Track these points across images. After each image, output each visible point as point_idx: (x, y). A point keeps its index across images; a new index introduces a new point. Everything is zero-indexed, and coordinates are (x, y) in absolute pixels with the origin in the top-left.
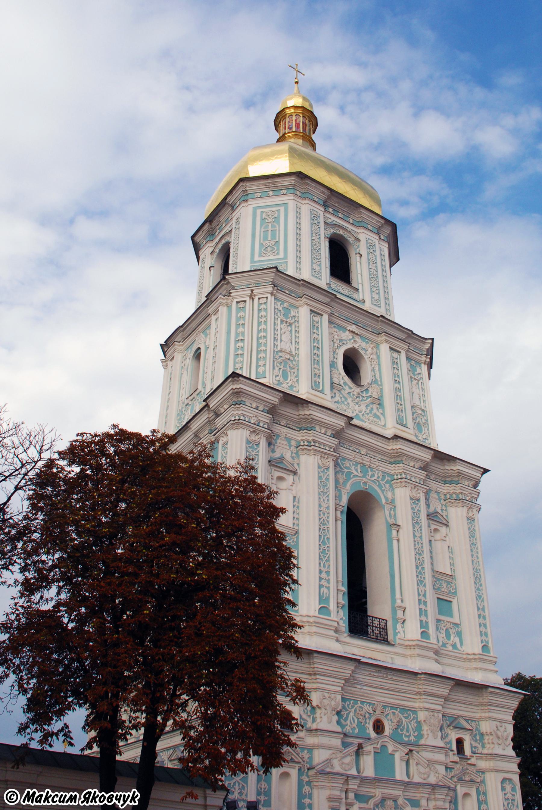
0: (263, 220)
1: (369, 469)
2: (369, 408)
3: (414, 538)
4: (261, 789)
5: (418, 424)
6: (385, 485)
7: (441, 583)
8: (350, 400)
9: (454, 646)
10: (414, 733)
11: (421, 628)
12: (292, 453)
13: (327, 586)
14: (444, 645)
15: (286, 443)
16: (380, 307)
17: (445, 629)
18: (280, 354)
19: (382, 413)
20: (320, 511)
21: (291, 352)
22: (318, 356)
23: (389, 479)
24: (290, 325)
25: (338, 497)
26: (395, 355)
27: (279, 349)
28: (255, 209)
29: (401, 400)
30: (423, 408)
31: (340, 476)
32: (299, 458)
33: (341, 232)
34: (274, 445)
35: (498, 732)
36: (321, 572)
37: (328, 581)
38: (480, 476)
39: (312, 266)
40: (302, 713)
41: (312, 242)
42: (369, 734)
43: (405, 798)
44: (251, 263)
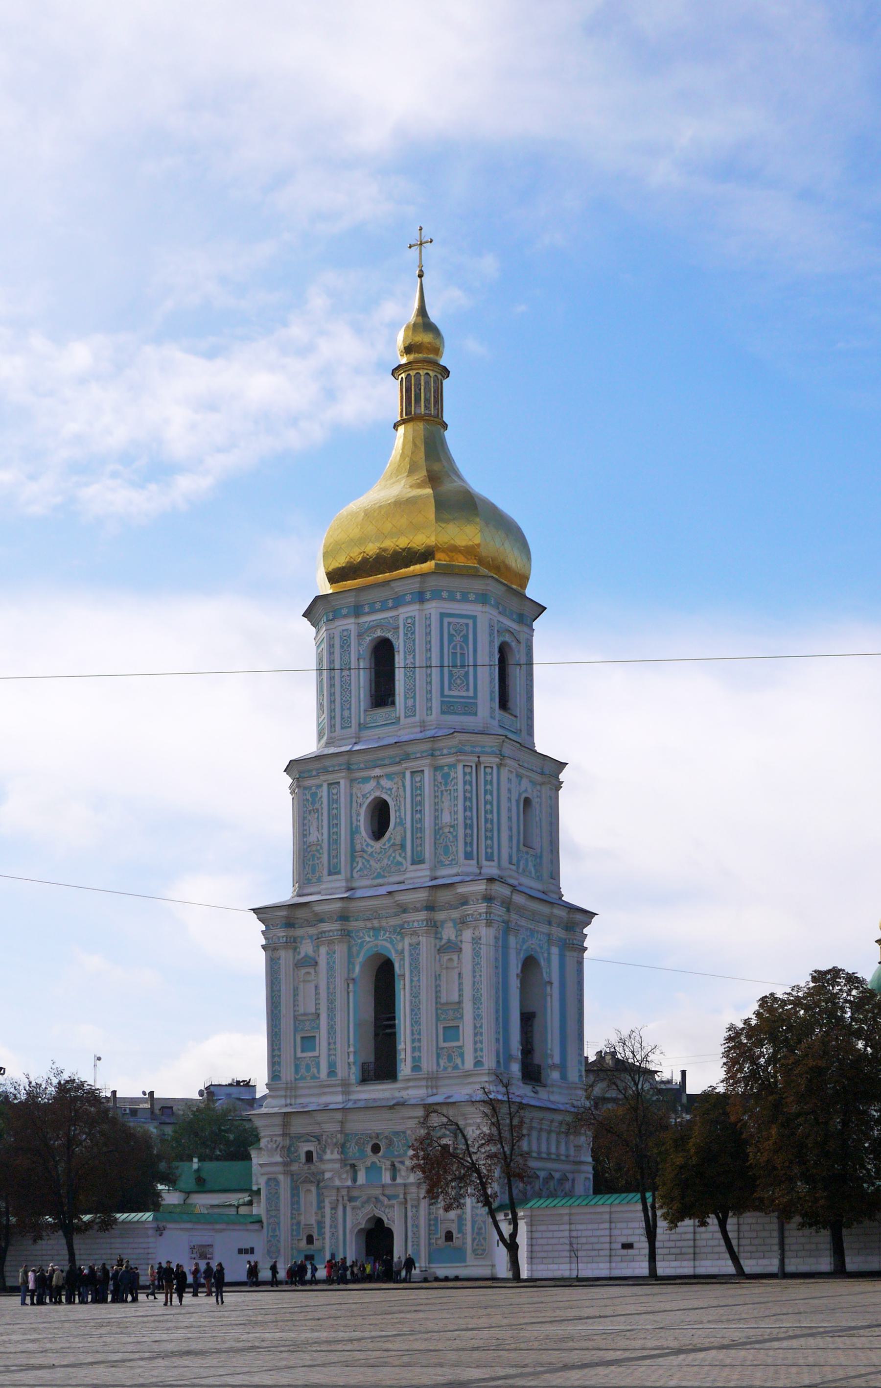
2: (392, 858)
8: (372, 863)
9: (456, 1067)
14: (445, 1069)
15: (309, 941)
16: (415, 715)
20: (328, 993)
21: (318, 841)
24: (318, 810)
26: (418, 779)
27: (308, 844)
31: (355, 949)
33: (379, 633)
36: (329, 1044)
37: (335, 1049)
39: (342, 715)
41: (342, 681)
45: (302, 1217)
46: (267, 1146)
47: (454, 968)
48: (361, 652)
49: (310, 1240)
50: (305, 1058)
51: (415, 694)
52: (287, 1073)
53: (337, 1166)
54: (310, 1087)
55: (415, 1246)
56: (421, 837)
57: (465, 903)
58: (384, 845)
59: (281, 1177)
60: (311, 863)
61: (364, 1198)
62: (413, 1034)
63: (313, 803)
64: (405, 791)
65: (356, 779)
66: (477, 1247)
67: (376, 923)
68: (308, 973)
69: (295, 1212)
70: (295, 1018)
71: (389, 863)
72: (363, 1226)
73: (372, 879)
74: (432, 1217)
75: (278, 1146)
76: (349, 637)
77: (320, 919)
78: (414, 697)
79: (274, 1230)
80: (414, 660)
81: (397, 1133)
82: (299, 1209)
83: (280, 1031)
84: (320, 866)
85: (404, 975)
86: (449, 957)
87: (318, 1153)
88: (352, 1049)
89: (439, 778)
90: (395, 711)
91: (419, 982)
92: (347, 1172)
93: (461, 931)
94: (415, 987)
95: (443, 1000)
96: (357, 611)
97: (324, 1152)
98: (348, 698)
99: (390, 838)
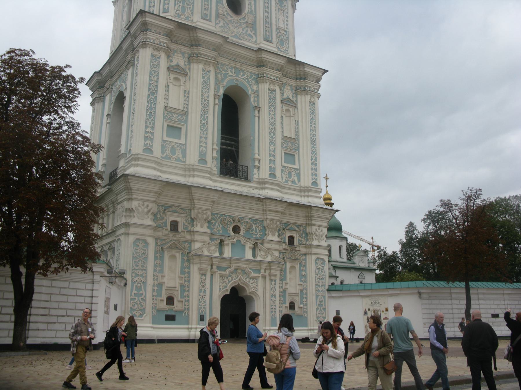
3: (269, 115)
4: (157, 264)
5: (282, 40)
7: (287, 144)
8: (230, 26)
9: (293, 182)
10: (260, 232)
12: (185, 62)
14: (287, 181)
15: (181, 55)
17: (288, 172)
19: (254, 34)
20: (202, 99)
25: (217, 89)
29: (269, 24)
30: (285, 29)
31: (219, 76)
32: (190, 65)
34: (172, 57)
35: (317, 232)
36: (201, 137)
37: (206, 143)
38: (321, 74)
40: (185, 222)
42: (230, 233)
43: (250, 269)
45: (165, 280)
46: (138, 210)
47: (291, 116)
49: (170, 300)
53: (207, 238)
54: (174, 167)
55: (274, 312)
56: (268, 27)
57: (305, 79)
58: (240, 20)
61: (233, 268)
62: (270, 151)
66: (319, 315)
67: (238, 65)
68: (176, 79)
69: (157, 274)
71: (244, 32)
72: (228, 293)
74: (281, 290)
77: (195, 43)
79: (138, 289)
81: (254, 220)
82: (161, 271)
85: (257, 108)
86: (287, 108)
87: (184, 224)
88: (215, 147)
91: (275, 116)
93: (296, 94)
94: (272, 118)
99: (244, 18)
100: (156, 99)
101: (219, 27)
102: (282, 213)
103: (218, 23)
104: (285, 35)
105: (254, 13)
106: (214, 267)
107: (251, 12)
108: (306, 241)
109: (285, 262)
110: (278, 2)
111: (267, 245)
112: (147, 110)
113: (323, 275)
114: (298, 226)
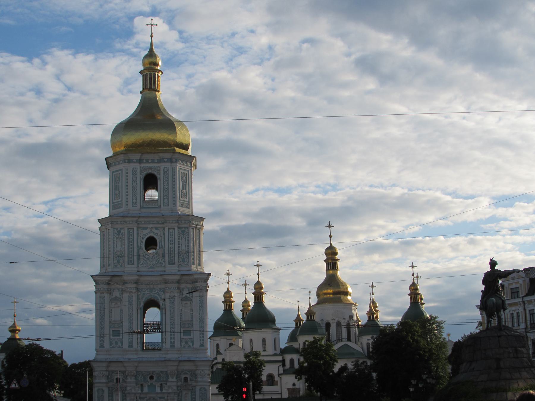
0: (115, 179)
1: (154, 289)
2: (157, 261)
6: (161, 293)
8: (148, 262)
9: (189, 346)
11: (171, 344)
12: (120, 293)
13: (132, 338)
14: (184, 347)
16: (168, 206)
18: (116, 253)
19: (163, 261)
20: (129, 313)
21: (121, 250)
22: (132, 248)
23: (163, 290)
24: (121, 238)
27: (116, 251)
28: (113, 172)
30: (186, 250)
33: (150, 171)
39: (133, 201)
41: (132, 188)
44: (113, 203)
48: (142, 178)
50: (115, 339)
51: (168, 197)
52: (107, 345)
53: (134, 384)
59: (104, 389)
60: (117, 259)
63: (119, 235)
64: (164, 234)
65: (140, 228)
67: (152, 286)
68: (116, 304)
70: (110, 322)
73: (148, 268)
75: (104, 375)
76: (137, 171)
77: (125, 283)
78: (168, 199)
80: (168, 184)
81: (162, 372)
83: (104, 327)
84: (122, 261)
87: (122, 379)
89: (180, 232)
90: (158, 204)
92: (139, 387)
94: (172, 314)
95: (183, 319)
96: (140, 161)
97: (126, 377)
98: (135, 195)
100: (104, 320)
101: (141, 265)
102: (178, 366)
103: (140, 263)
104: (186, 254)
105: (164, 247)
106: (138, 398)
107: (162, 247)
108: (196, 379)
109: (182, 392)
110: (181, 233)
111: (168, 384)
112: (100, 326)
113: (205, 397)
114: (189, 371)
